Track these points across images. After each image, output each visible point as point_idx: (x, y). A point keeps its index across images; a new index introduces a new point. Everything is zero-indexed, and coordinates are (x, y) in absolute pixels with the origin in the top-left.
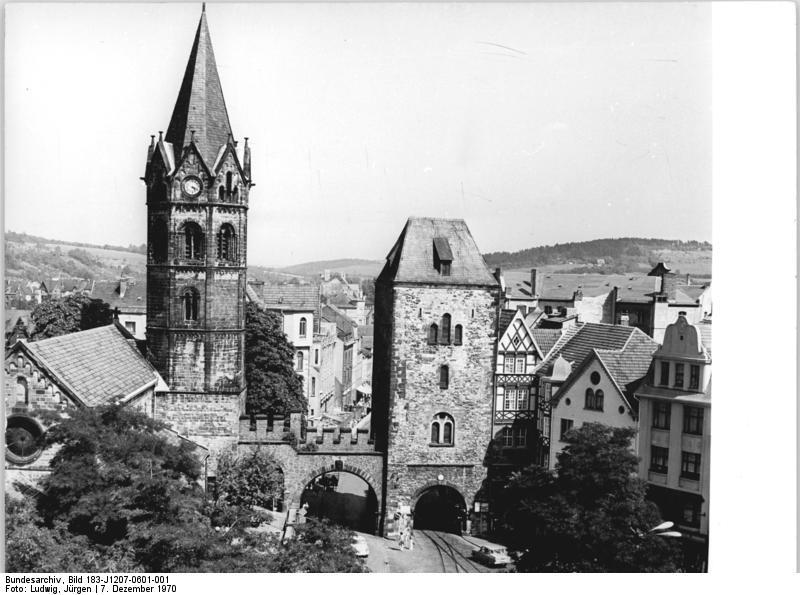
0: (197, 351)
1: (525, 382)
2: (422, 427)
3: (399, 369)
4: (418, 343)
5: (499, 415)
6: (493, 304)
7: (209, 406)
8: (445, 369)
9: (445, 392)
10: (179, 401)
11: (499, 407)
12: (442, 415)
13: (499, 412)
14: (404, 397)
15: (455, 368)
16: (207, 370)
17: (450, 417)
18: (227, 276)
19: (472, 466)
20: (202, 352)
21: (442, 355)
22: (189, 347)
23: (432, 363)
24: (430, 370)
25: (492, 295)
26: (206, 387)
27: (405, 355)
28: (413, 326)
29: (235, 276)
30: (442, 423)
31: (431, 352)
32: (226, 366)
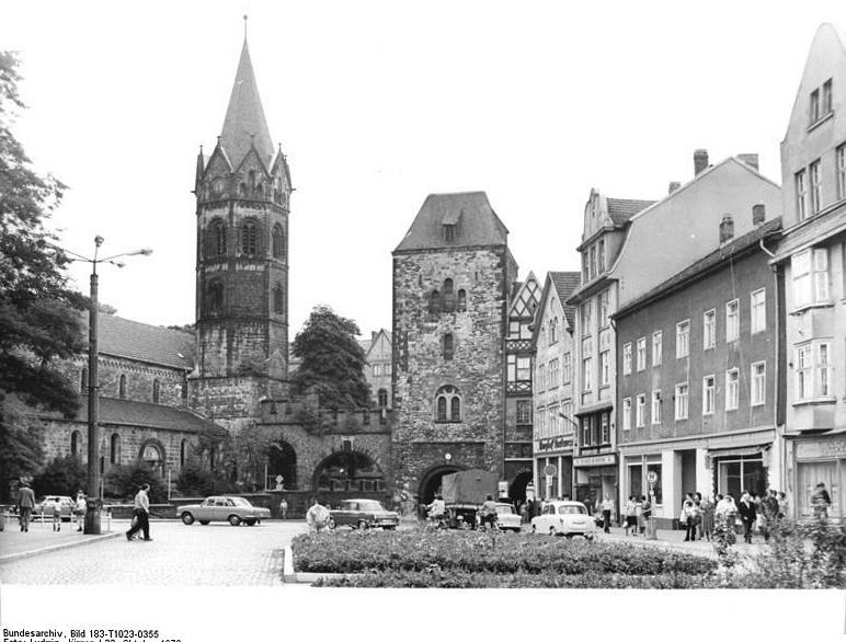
0: (221, 338)
1: (523, 348)
2: (426, 402)
4: (420, 312)
5: (511, 387)
6: (499, 266)
8: (448, 338)
9: (449, 363)
12: (448, 388)
14: (406, 370)
15: (461, 337)
16: (229, 355)
17: (457, 390)
18: (252, 267)
19: (484, 443)
20: (225, 339)
22: (216, 334)
23: (434, 333)
24: (432, 339)
26: (229, 371)
27: (407, 326)
29: (261, 268)
30: (448, 396)
31: (432, 321)
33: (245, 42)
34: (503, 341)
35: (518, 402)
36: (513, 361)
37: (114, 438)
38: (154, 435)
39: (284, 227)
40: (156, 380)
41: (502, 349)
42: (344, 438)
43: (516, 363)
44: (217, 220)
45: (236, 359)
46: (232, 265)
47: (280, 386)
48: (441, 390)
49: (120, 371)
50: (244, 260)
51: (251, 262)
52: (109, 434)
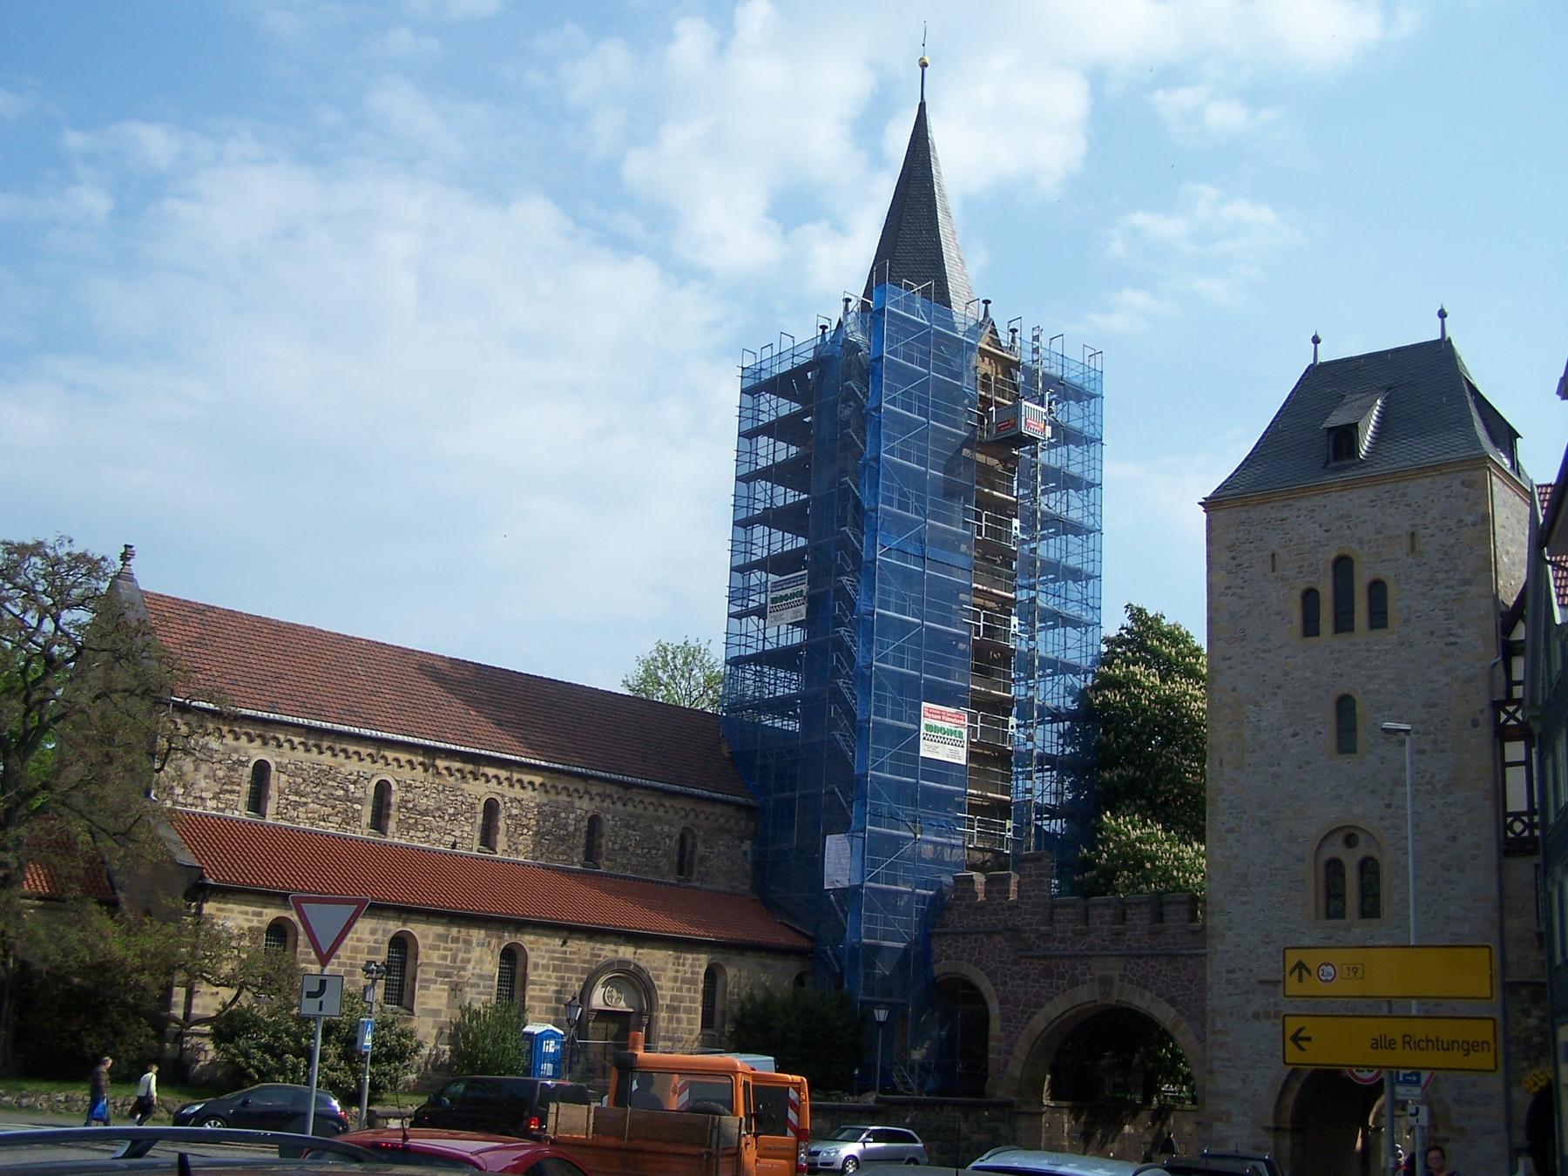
11: (1517, 800)
13: (1517, 816)
34: (1497, 706)
36: (1522, 758)
37: (512, 959)
38: (626, 952)
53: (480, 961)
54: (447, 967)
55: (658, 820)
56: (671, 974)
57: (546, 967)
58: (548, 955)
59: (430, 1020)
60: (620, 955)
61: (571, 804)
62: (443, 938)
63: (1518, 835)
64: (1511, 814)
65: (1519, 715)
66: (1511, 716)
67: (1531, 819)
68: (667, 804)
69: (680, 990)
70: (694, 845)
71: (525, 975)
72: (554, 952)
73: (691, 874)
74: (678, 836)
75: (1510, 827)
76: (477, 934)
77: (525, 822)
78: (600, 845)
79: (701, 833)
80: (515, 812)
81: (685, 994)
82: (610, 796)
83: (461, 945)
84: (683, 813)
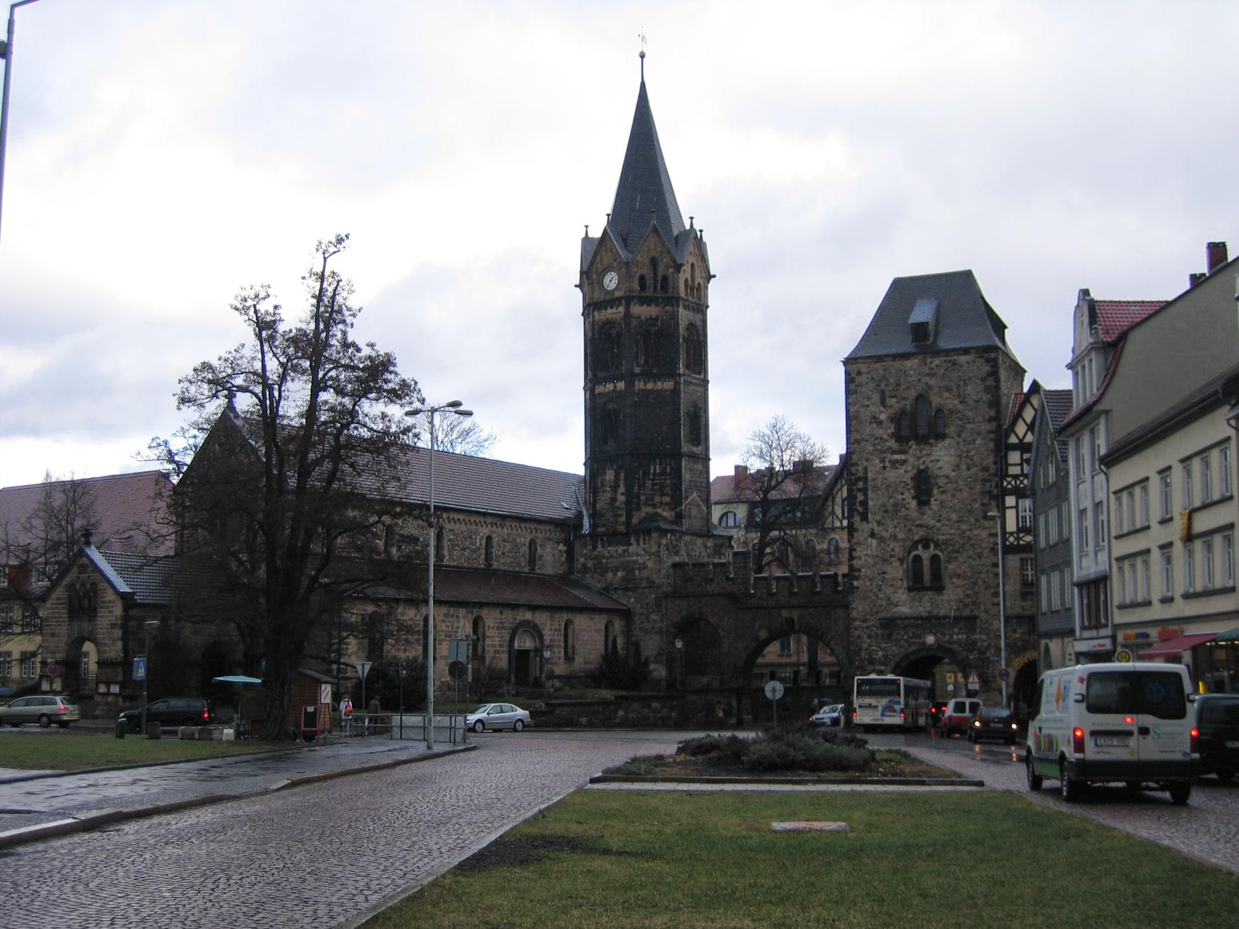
2: (898, 564)
3: (859, 479)
7: (633, 549)
10: (600, 546)
11: (1011, 526)
12: (925, 543)
13: (1011, 534)
16: (628, 503)
19: (975, 618)
21: (915, 457)
22: (610, 475)
24: (904, 474)
25: (988, 361)
26: (628, 523)
28: (874, 417)
29: (669, 385)
31: (903, 452)
32: (657, 499)
33: (643, 85)
35: (1022, 560)
36: (1014, 504)
37: (477, 623)
38: (528, 616)
39: (700, 328)
40: (532, 542)
41: (997, 487)
42: (785, 613)
43: (1017, 507)
44: (609, 323)
45: (638, 509)
46: (630, 384)
47: (699, 541)
48: (915, 546)
49: (485, 531)
50: (648, 376)
51: (656, 377)
52: (471, 617)
53: (464, 627)
54: (449, 631)
55: (518, 535)
56: (549, 627)
57: (493, 628)
58: (494, 621)
59: (444, 662)
60: (526, 618)
61: (478, 530)
62: (447, 615)
63: (1012, 544)
64: (1009, 533)
65: (1013, 483)
66: (1009, 483)
67: (1018, 535)
68: (523, 526)
69: (554, 635)
70: (536, 549)
71: (484, 633)
72: (496, 619)
73: (535, 564)
74: (528, 545)
75: (1007, 539)
76: (462, 612)
77: (456, 542)
78: (492, 553)
79: (539, 541)
80: (451, 537)
81: (556, 637)
82: (496, 524)
83: (455, 619)
84: (529, 531)
